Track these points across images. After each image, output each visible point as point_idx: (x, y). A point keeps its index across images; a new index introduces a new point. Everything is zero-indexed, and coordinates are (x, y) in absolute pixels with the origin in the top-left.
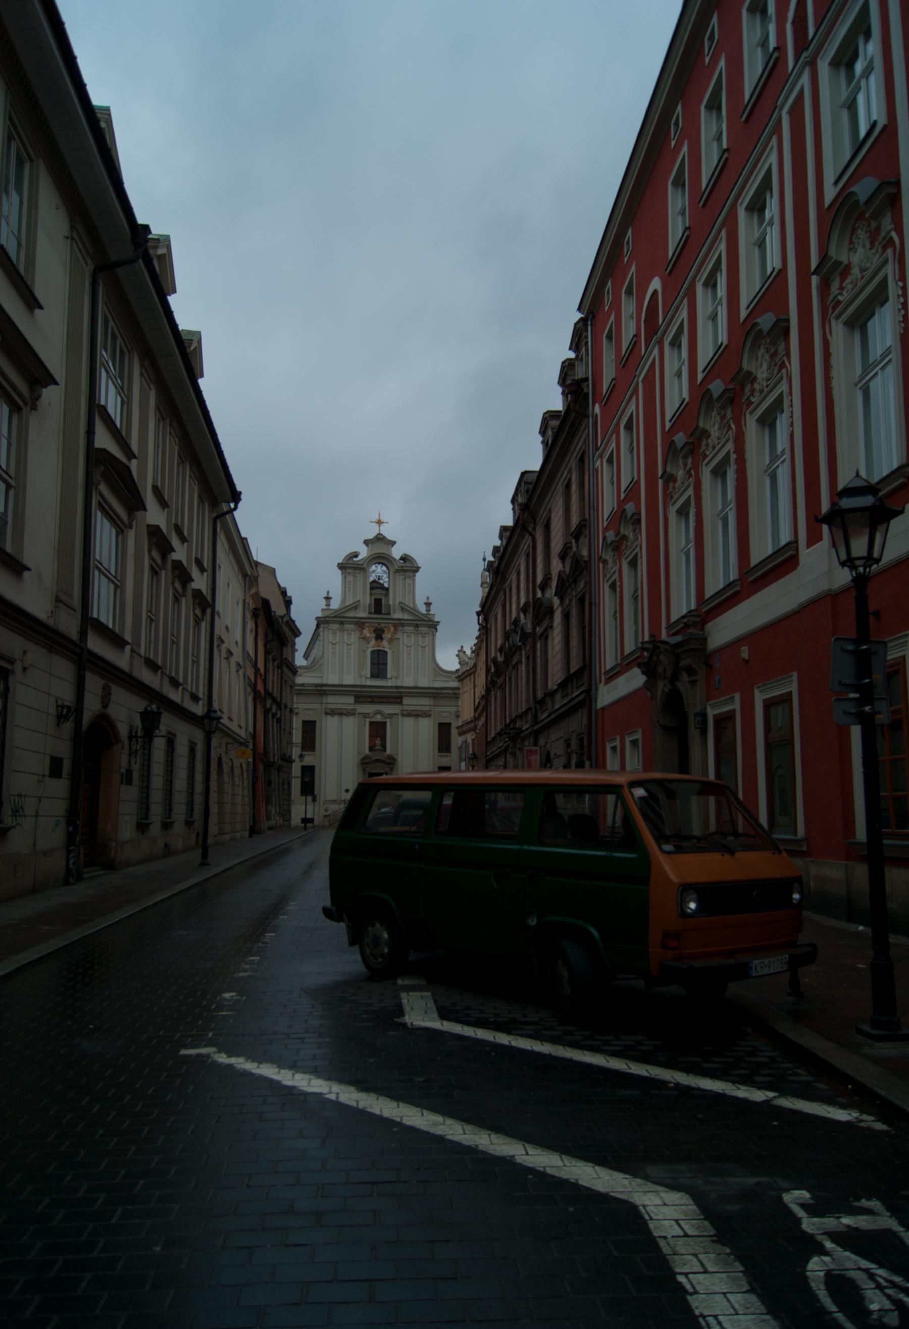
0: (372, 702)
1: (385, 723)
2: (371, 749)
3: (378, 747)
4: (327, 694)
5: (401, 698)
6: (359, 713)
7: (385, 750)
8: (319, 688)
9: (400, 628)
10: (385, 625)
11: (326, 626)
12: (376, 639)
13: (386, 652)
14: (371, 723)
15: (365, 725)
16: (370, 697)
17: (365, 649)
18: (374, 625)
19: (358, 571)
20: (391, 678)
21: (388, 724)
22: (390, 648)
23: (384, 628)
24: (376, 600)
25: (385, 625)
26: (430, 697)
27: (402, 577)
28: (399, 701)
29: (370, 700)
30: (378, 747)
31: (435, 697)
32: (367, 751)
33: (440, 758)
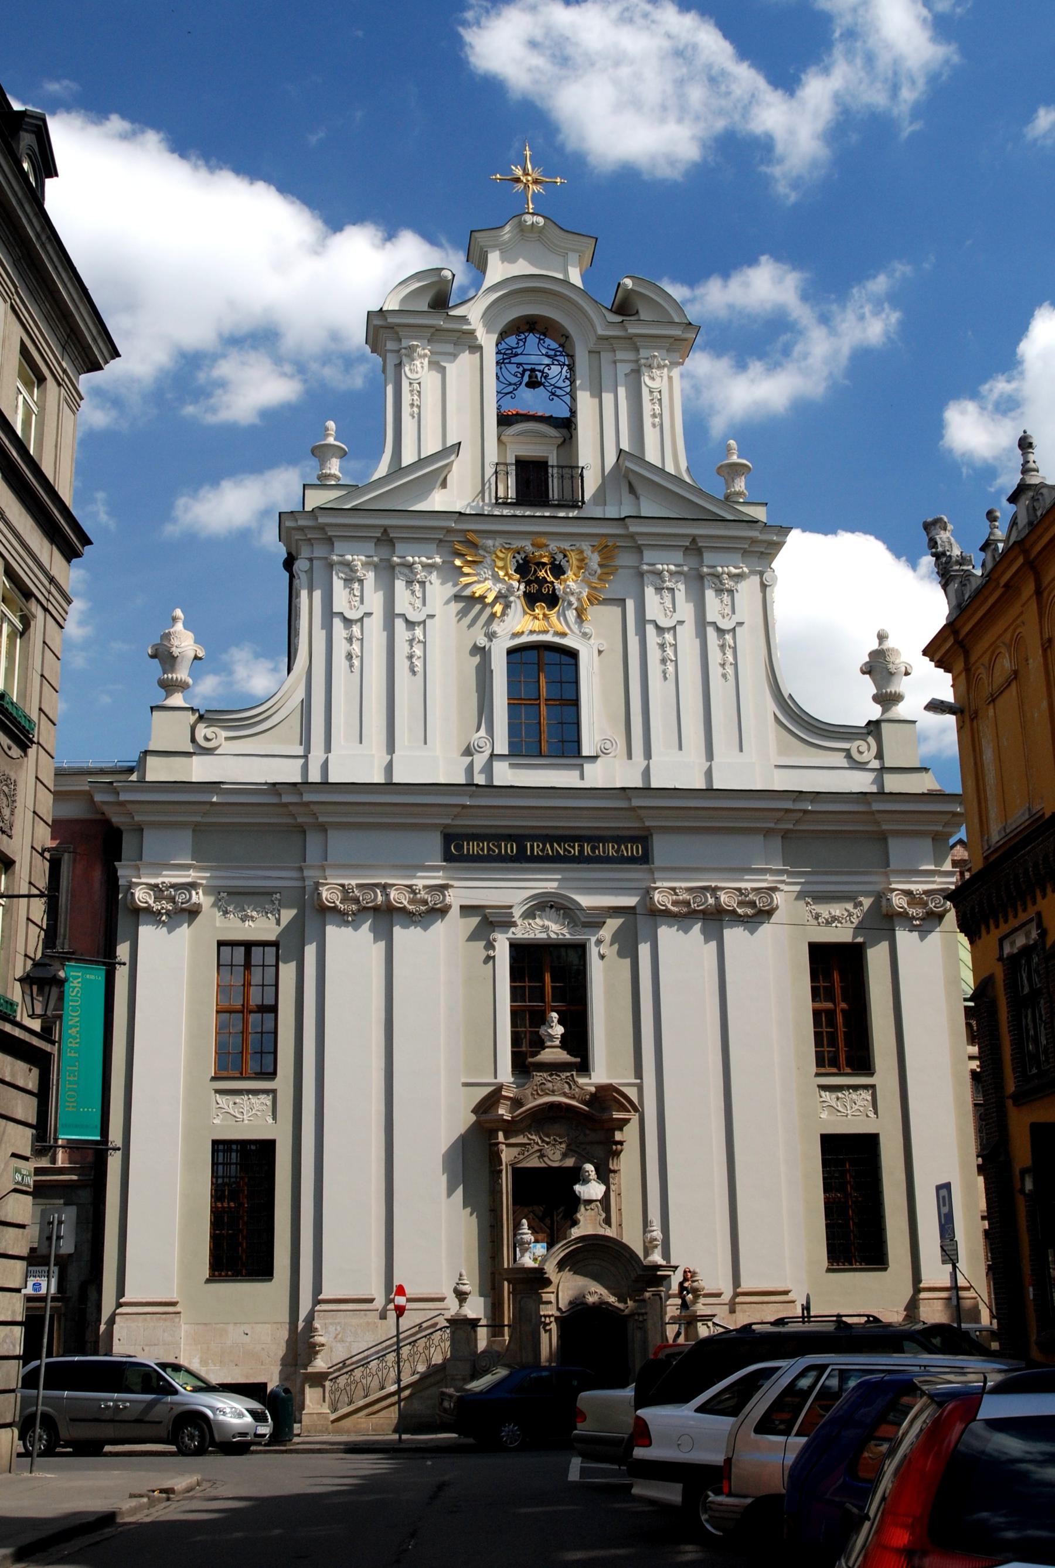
0: (522, 858)
1: (580, 949)
2: (521, 1066)
3: (553, 1054)
4: (323, 828)
5: (644, 839)
6: (467, 910)
7: (584, 1067)
8: (286, 799)
9: (625, 559)
10: (565, 545)
11: (319, 551)
12: (531, 599)
13: (572, 655)
14: (517, 948)
15: (490, 959)
16: (519, 839)
17: (482, 641)
18: (517, 544)
19: (450, 348)
20: (594, 758)
21: (593, 952)
22: (585, 635)
23: (559, 557)
24: (522, 465)
25: (565, 545)
26: (768, 833)
27: (623, 369)
28: (637, 850)
29: (512, 848)
30: (553, 1054)
31: (786, 835)
32: (505, 1074)
33: (826, 1095)
